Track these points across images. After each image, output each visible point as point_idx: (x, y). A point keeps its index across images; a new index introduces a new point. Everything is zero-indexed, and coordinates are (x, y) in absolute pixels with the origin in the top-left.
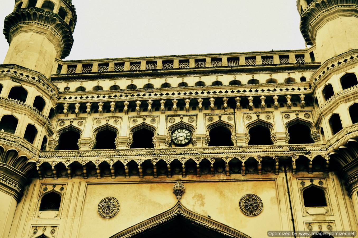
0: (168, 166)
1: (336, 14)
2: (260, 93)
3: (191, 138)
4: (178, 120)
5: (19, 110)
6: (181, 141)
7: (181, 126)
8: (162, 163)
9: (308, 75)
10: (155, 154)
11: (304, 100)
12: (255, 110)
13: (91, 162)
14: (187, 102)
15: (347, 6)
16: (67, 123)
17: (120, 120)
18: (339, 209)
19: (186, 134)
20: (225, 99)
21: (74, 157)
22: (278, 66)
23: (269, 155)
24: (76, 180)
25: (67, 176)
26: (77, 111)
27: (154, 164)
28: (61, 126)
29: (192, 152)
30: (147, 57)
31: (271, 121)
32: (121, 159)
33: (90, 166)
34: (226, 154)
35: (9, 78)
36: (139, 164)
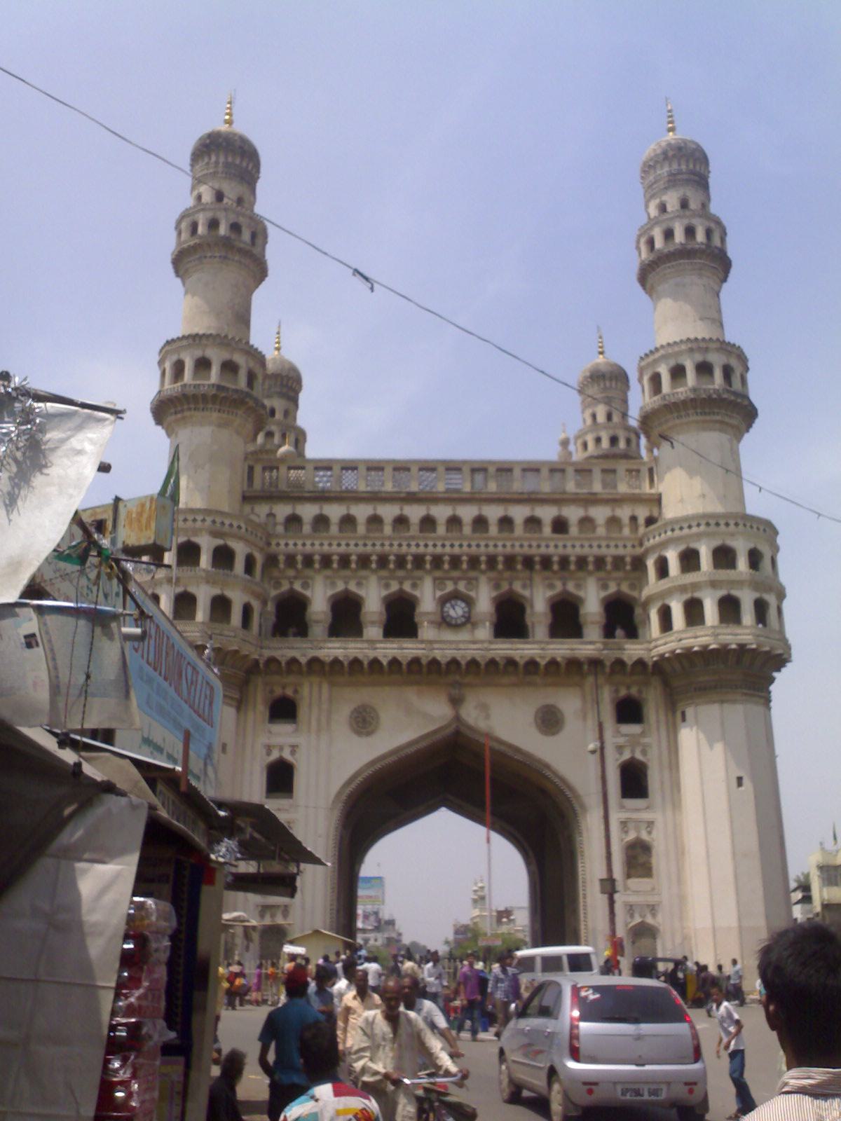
2: (569, 551)
4: (450, 587)
6: (456, 619)
7: (455, 596)
8: (434, 662)
16: (285, 587)
17: (364, 582)
18: (658, 728)
21: (312, 649)
23: (577, 656)
24: (315, 679)
25: (300, 672)
26: (300, 566)
31: (581, 594)
33: (336, 662)
34: (521, 650)
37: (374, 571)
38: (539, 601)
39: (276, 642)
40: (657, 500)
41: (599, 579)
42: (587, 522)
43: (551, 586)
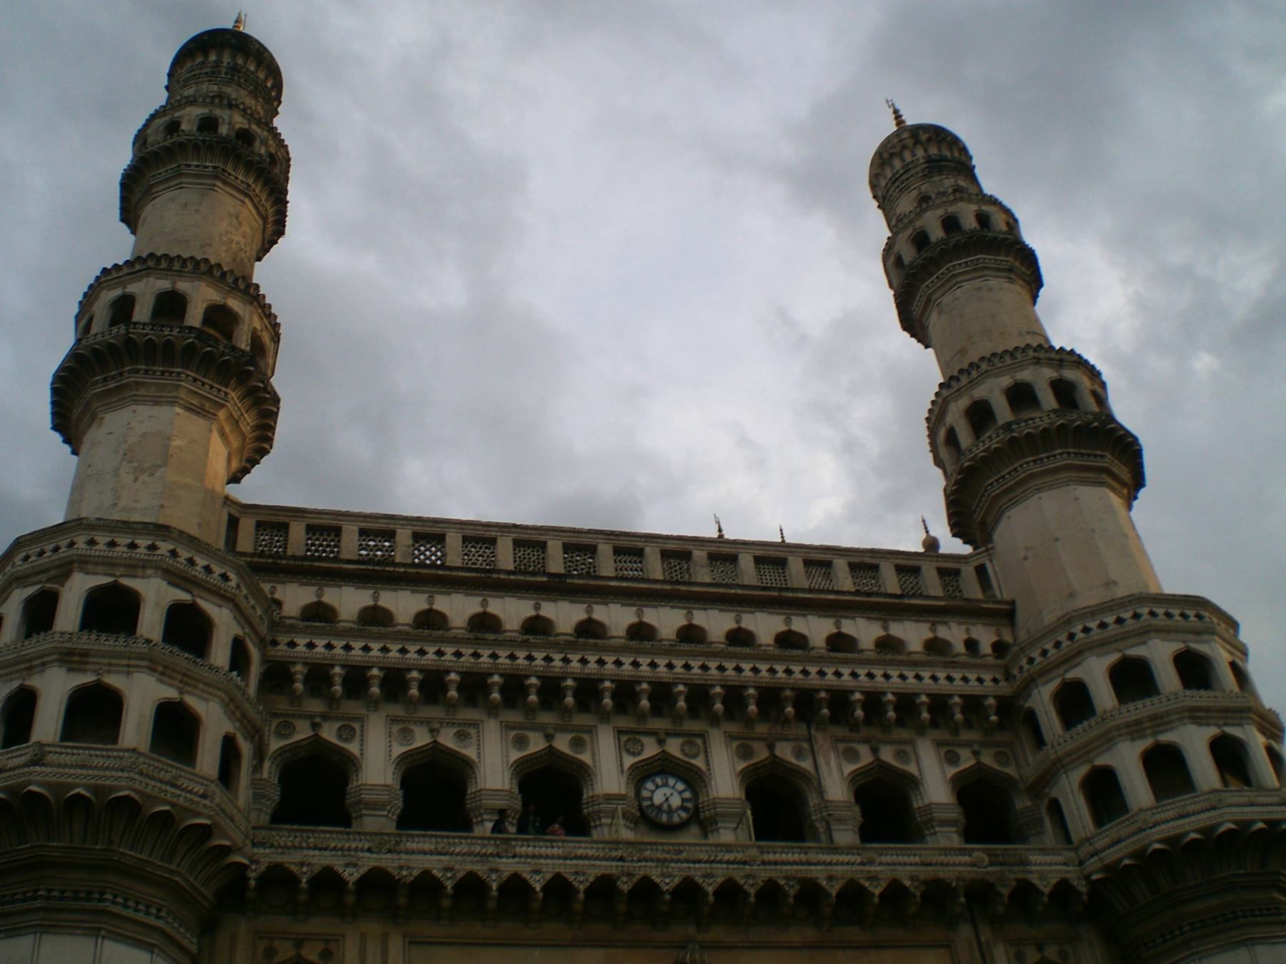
0: (668, 897)
1: (1062, 475)
3: (696, 809)
4: (650, 749)
5: (201, 686)
7: (663, 767)
8: (646, 889)
9: (986, 637)
10: (621, 859)
11: (996, 714)
12: (865, 732)
13: (426, 873)
14: (680, 693)
15: (1089, 455)
16: (302, 732)
17: (473, 732)
19: (680, 793)
20: (788, 693)
21: (369, 850)
22: (906, 601)
24: (372, 928)
27: (625, 888)
28: (280, 735)
29: (731, 857)
30: (515, 526)
31: (912, 768)
32: (524, 870)
33: (426, 885)
35: (160, 573)
36: (582, 887)
37: (492, 710)
38: (834, 779)
39: (284, 836)
40: (1006, 614)
41: (939, 744)
42: (888, 645)
43: (852, 755)
